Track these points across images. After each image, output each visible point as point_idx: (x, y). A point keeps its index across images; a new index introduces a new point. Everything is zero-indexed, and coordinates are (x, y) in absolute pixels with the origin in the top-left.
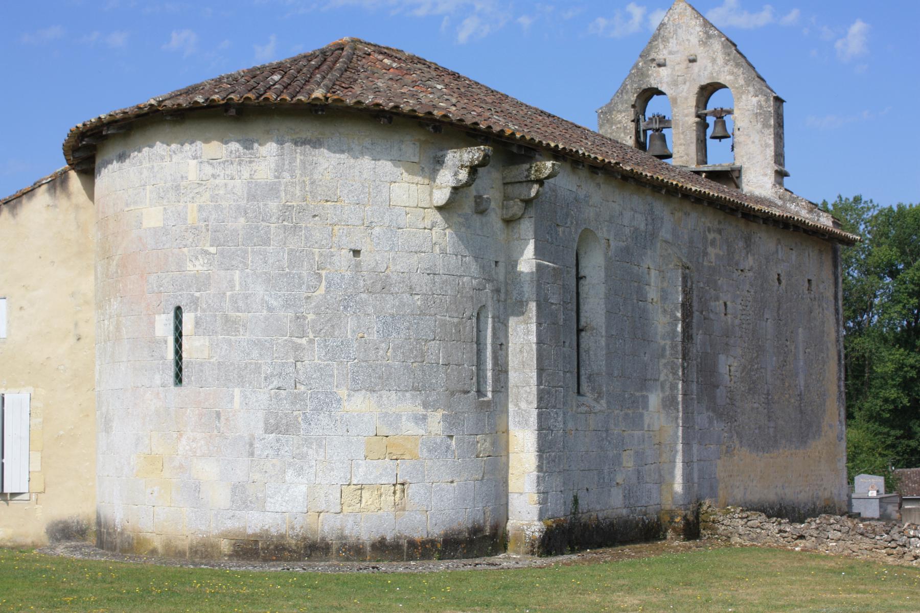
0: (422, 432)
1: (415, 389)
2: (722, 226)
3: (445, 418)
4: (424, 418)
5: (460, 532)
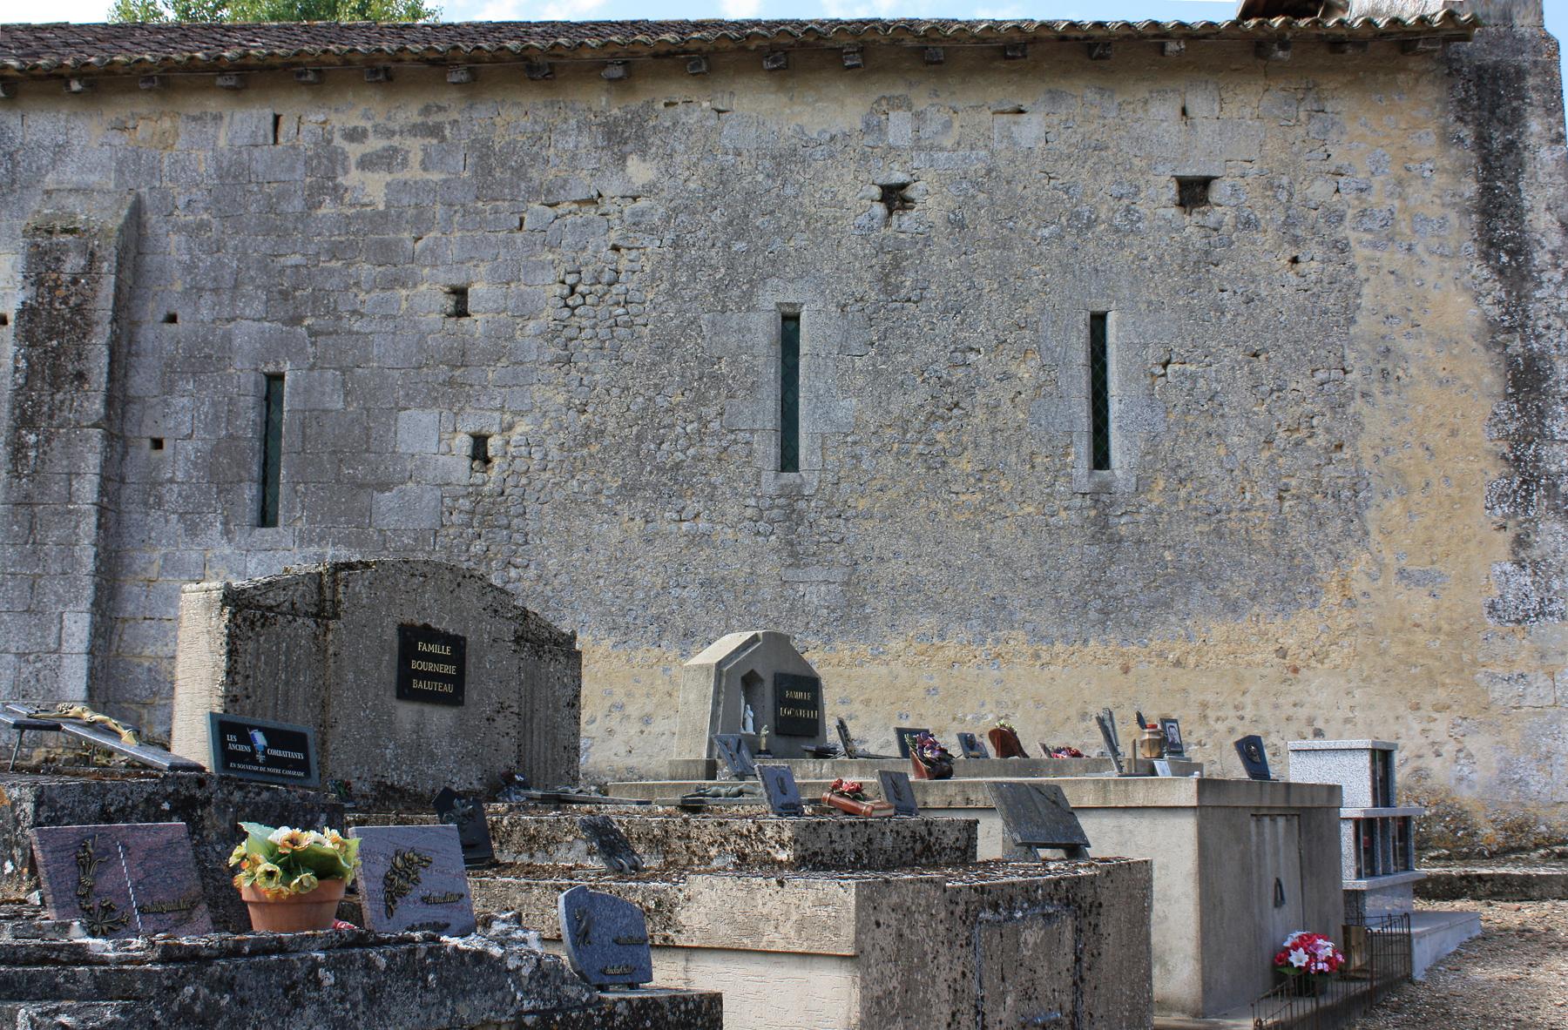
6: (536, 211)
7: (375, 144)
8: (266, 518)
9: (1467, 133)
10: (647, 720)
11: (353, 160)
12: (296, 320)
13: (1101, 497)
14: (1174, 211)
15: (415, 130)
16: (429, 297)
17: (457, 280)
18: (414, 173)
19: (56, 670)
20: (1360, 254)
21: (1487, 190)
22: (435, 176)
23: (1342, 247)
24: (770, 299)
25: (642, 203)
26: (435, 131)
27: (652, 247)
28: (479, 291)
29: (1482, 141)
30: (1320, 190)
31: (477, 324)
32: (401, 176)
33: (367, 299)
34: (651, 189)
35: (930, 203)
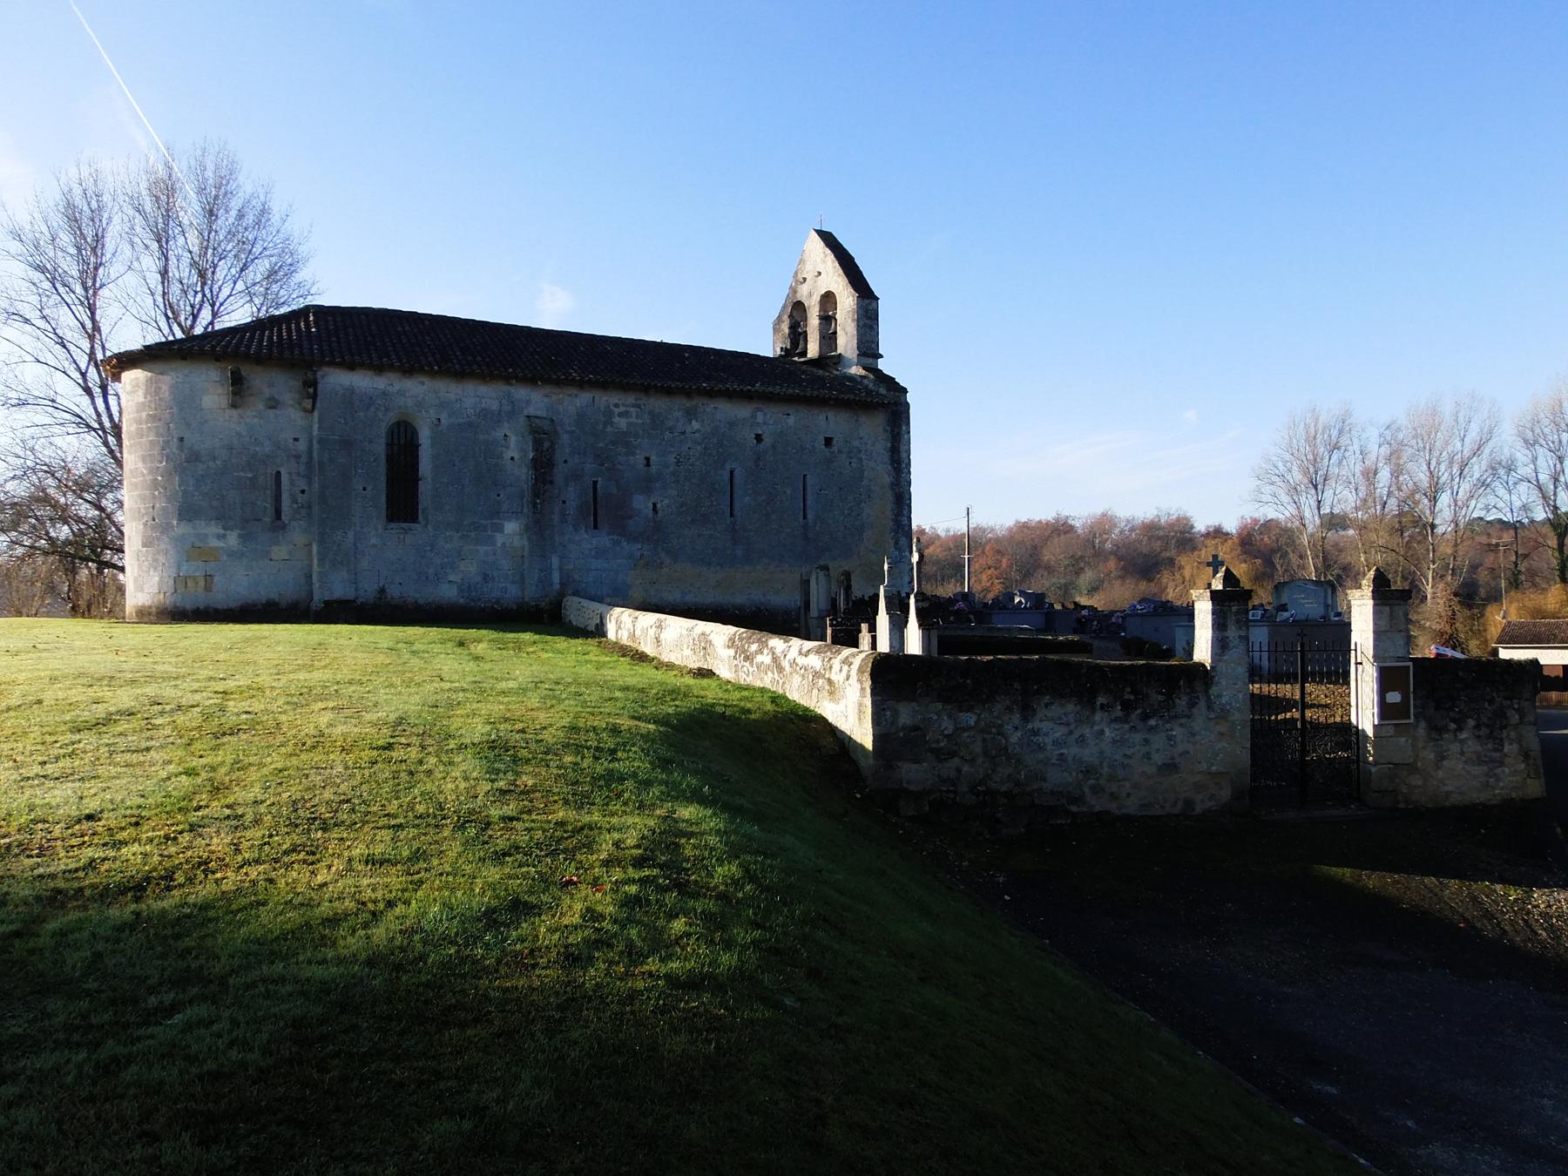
0: (222, 545)
1: (217, 519)
2: (639, 402)
3: (240, 536)
4: (224, 536)
5: (255, 605)
6: (668, 435)
7: (622, 409)
8: (596, 527)
9: (889, 429)
10: (699, 588)
11: (616, 413)
12: (603, 465)
13: (805, 527)
14: (823, 447)
15: (634, 406)
16: (639, 459)
17: (647, 455)
18: (633, 420)
19: (551, 574)
20: (865, 462)
21: (893, 446)
22: (640, 421)
23: (860, 460)
24: (728, 467)
25: (697, 435)
26: (639, 407)
27: (699, 448)
28: (653, 458)
29: (892, 431)
30: (856, 443)
31: (654, 469)
32: (631, 420)
33: (622, 459)
34: (698, 431)
35: (767, 441)
